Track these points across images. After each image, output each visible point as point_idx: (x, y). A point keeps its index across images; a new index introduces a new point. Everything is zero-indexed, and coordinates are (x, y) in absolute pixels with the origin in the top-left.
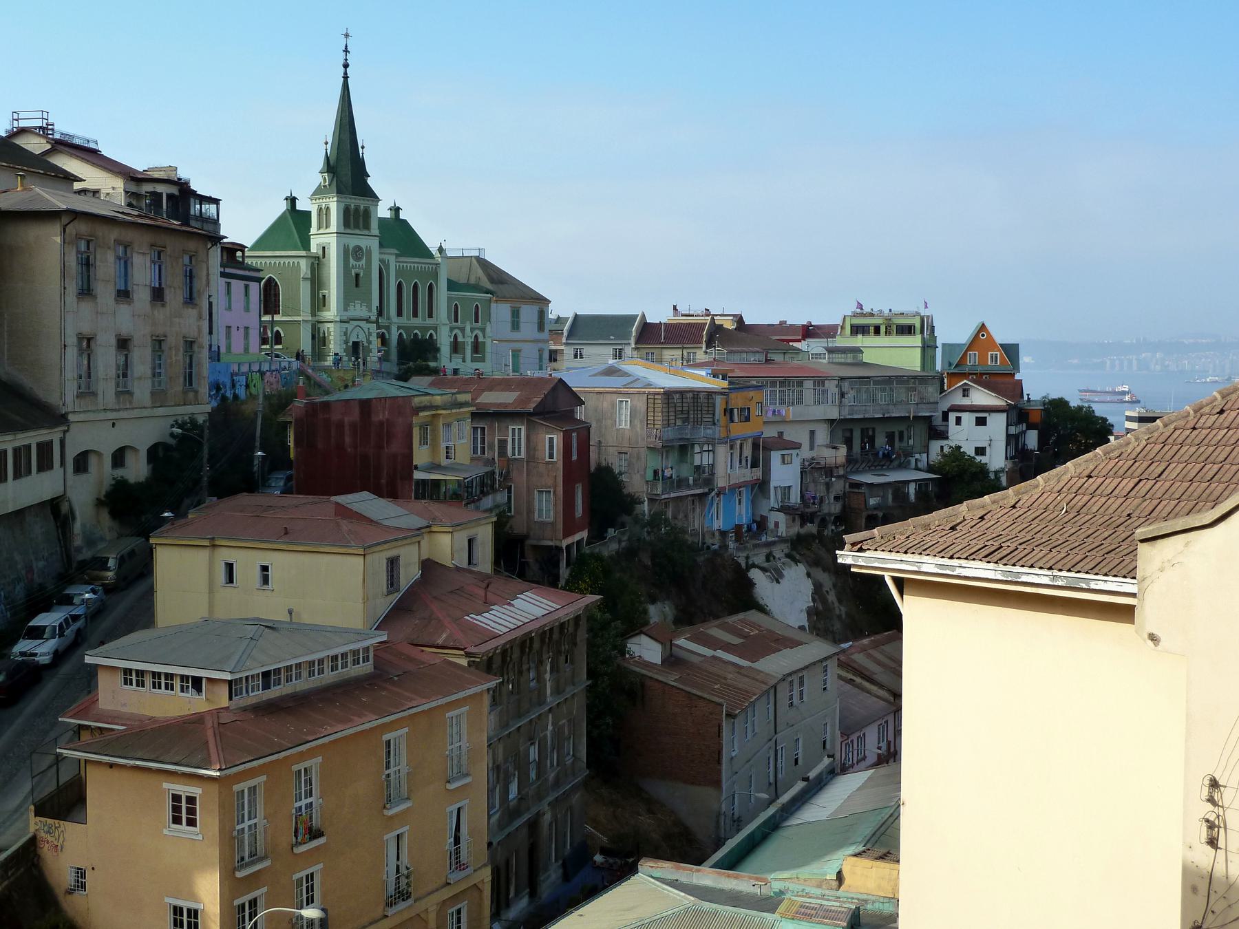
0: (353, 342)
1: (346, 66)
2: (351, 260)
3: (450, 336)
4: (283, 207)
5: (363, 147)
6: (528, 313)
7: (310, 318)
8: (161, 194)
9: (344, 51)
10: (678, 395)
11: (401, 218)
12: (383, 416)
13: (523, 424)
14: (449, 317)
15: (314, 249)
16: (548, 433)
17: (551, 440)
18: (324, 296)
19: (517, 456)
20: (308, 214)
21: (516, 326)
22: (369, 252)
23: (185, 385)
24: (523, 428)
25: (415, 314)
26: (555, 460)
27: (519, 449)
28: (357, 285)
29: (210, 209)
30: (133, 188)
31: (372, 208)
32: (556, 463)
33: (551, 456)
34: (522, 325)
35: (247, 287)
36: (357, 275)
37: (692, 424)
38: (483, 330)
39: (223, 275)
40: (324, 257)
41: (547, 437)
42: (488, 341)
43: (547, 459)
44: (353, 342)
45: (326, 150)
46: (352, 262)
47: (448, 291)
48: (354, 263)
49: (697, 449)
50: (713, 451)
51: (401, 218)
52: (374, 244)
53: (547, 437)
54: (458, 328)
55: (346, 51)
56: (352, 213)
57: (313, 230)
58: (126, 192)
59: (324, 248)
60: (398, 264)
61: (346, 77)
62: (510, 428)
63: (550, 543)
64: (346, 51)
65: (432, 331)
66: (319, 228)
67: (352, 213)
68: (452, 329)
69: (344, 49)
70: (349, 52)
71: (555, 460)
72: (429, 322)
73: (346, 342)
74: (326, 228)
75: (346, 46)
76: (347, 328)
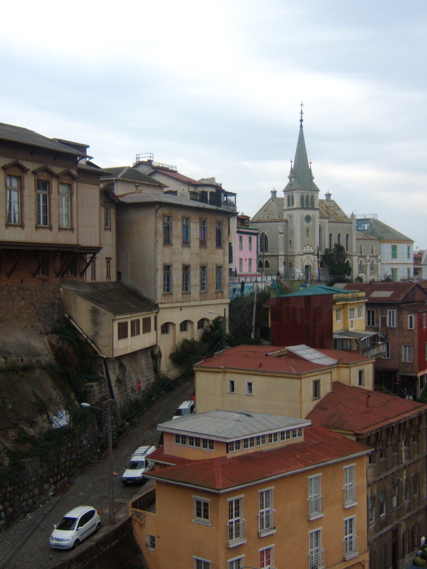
4: (270, 196)
5: (311, 163)
6: (402, 248)
7: (283, 253)
8: (206, 192)
13: (395, 309)
16: (409, 314)
17: (411, 318)
18: (291, 242)
19: (392, 326)
20: (283, 199)
21: (394, 255)
23: (183, 290)
24: (395, 311)
26: (413, 328)
27: (393, 322)
29: (232, 198)
30: (192, 189)
32: (413, 330)
33: (411, 326)
34: (398, 255)
35: (250, 238)
39: (238, 232)
41: (409, 316)
43: (409, 328)
45: (291, 165)
48: (306, 224)
52: (317, 213)
53: (409, 316)
55: (302, 113)
56: (305, 198)
58: (190, 192)
60: (329, 224)
61: (301, 126)
62: (388, 311)
63: (410, 374)
64: (302, 113)
66: (289, 206)
67: (305, 198)
69: (300, 112)
71: (413, 328)
73: (302, 266)
76: (302, 258)
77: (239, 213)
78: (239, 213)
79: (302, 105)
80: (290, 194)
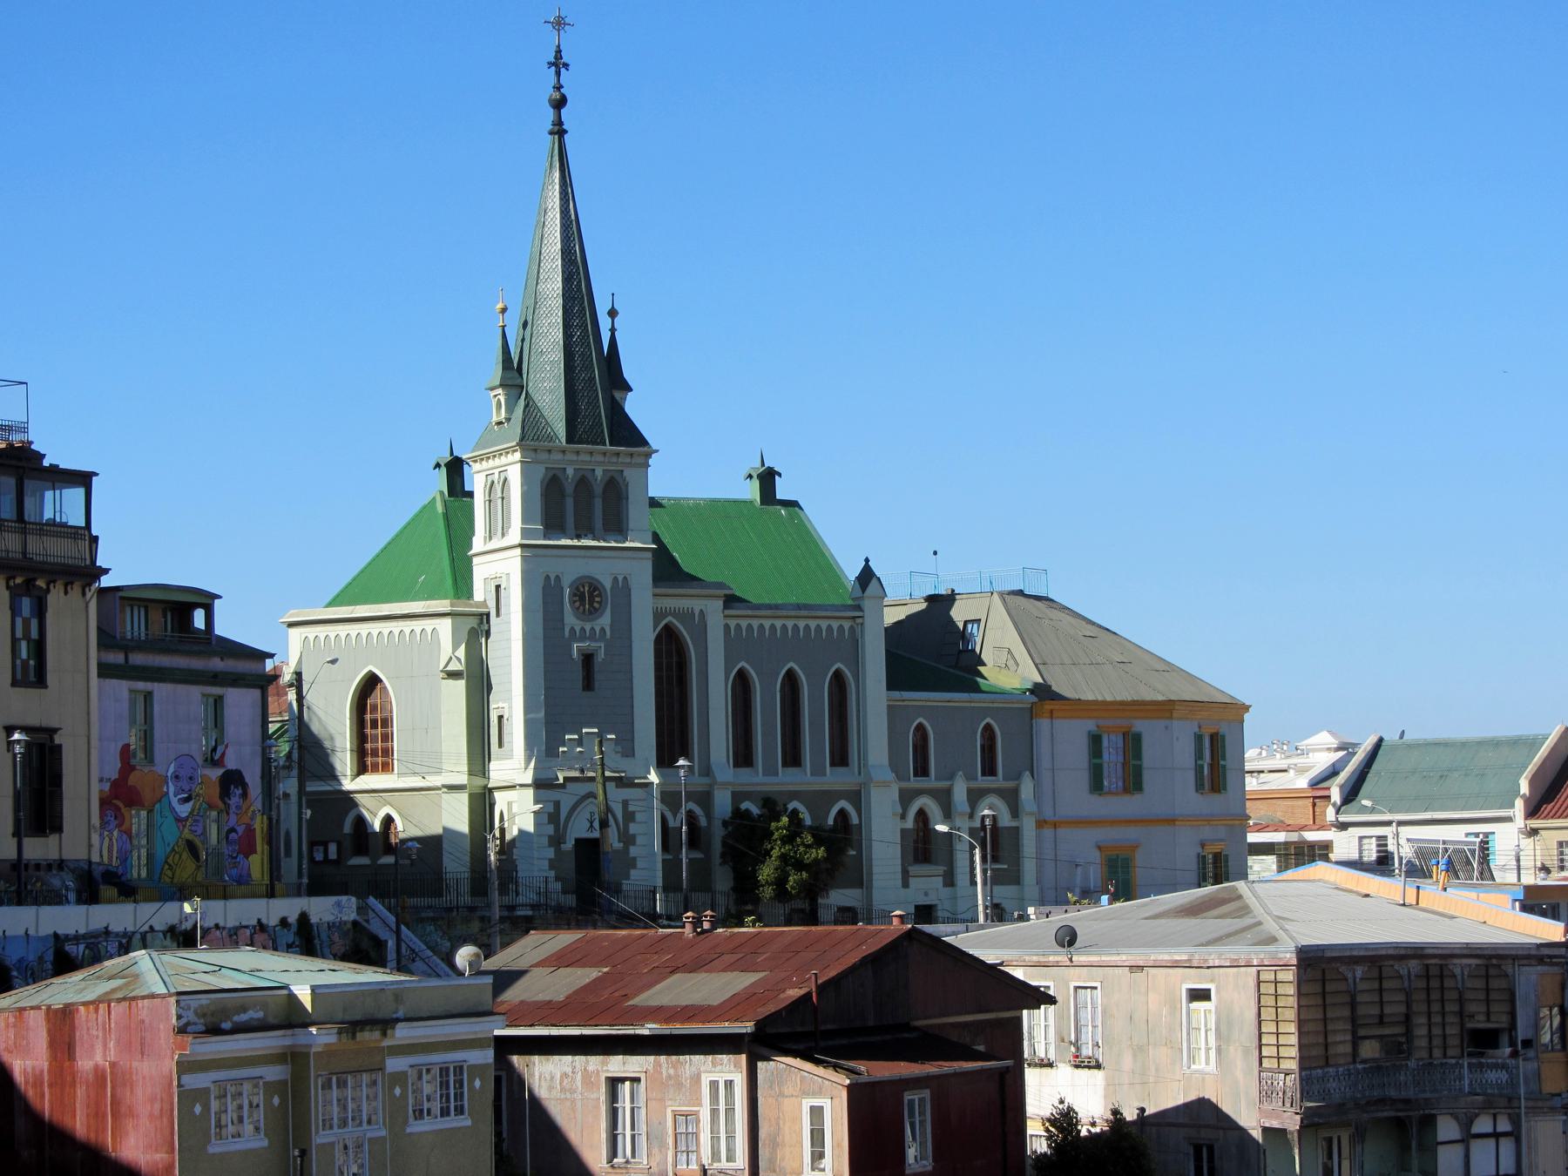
0: (577, 840)
1: (559, 103)
2: (570, 619)
3: (903, 817)
5: (613, 313)
7: (463, 779)
9: (550, 64)
10: (1359, 971)
11: (466, 489)
12: (105, 1055)
14: (895, 764)
15: (478, 596)
16: (806, 1093)
17: (817, 1112)
19: (724, 1164)
22: (623, 589)
25: (793, 757)
28: (588, 684)
31: (628, 473)
34: (1147, 776)
36: (588, 659)
37: (1424, 1054)
38: (1012, 798)
39: (106, 671)
40: (498, 615)
41: (807, 1103)
42: (1028, 827)
44: (577, 840)
46: (570, 619)
47: (891, 686)
49: (1447, 1128)
50: (1515, 1135)
51: (466, 489)
53: (807, 1103)
54: (999, 792)
55: (558, 64)
57: (478, 543)
59: (498, 587)
60: (732, 623)
64: (558, 64)
65: (843, 804)
67: (569, 489)
68: (906, 797)
70: (566, 66)
72: (835, 779)
73: (556, 841)
74: (503, 535)
75: (559, 52)
76: (557, 804)
77: (106, 571)
78: (106, 571)
79: (559, 24)
80: (496, 471)
